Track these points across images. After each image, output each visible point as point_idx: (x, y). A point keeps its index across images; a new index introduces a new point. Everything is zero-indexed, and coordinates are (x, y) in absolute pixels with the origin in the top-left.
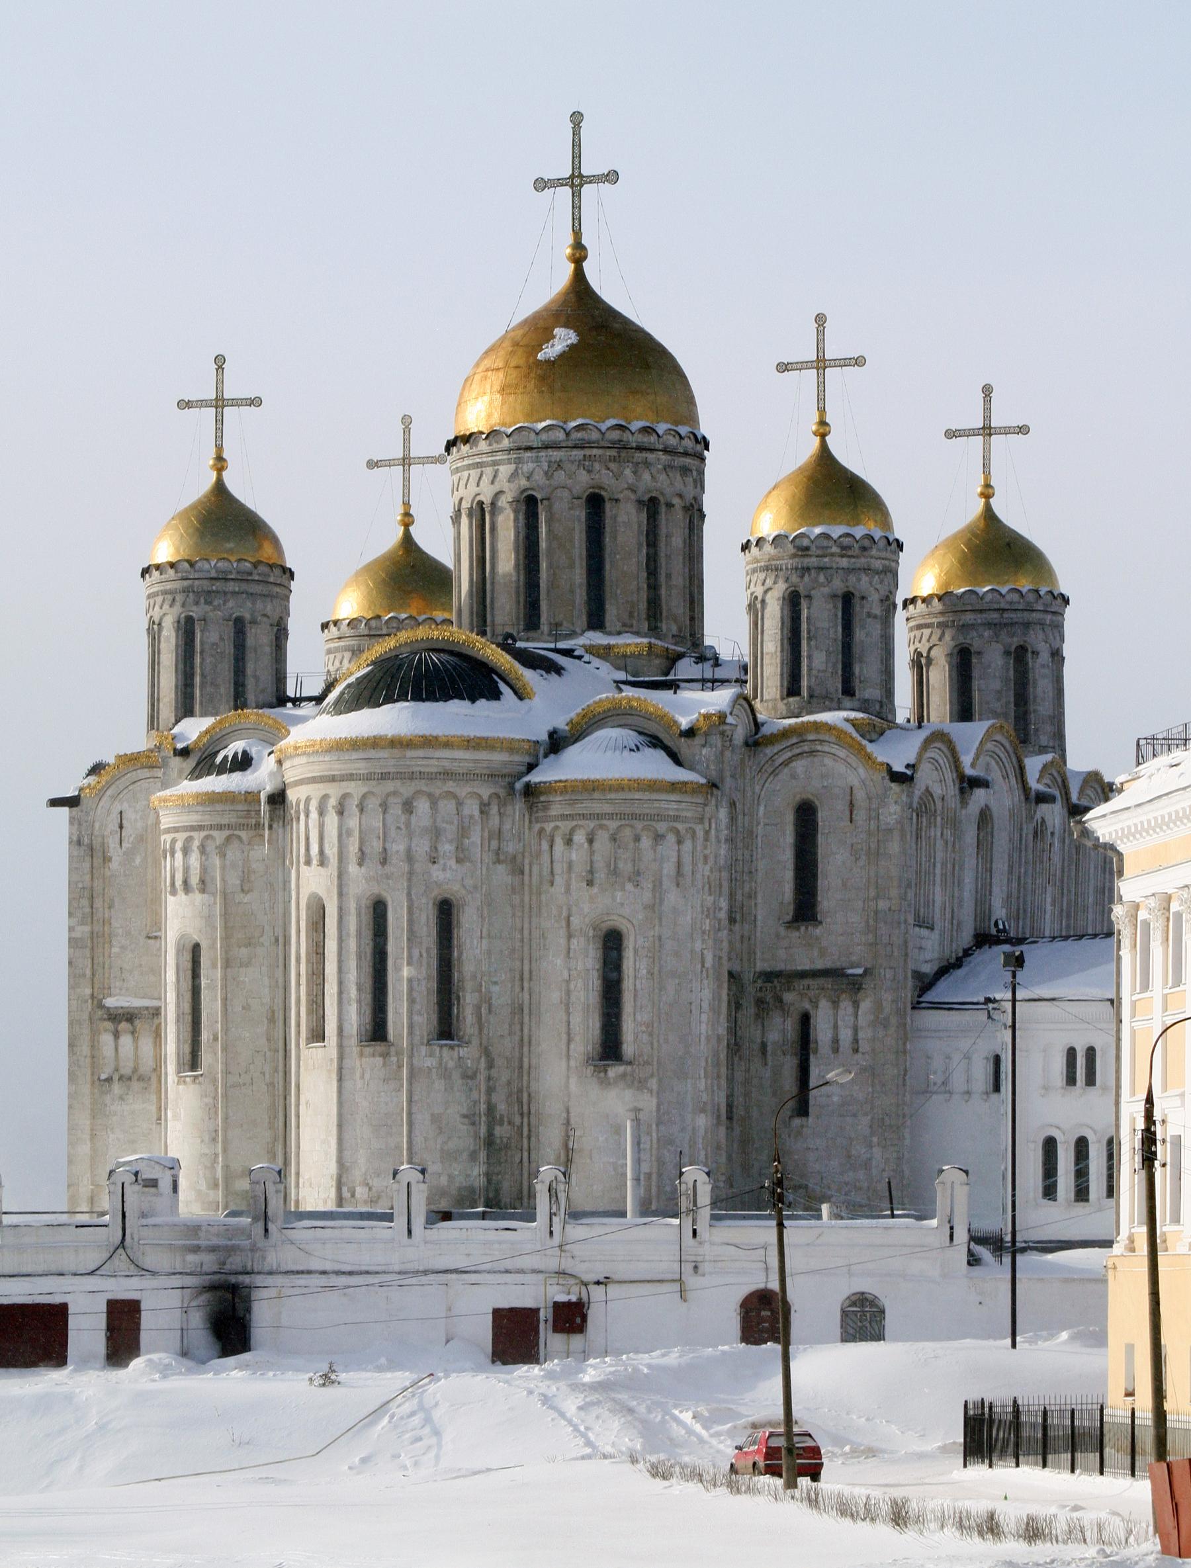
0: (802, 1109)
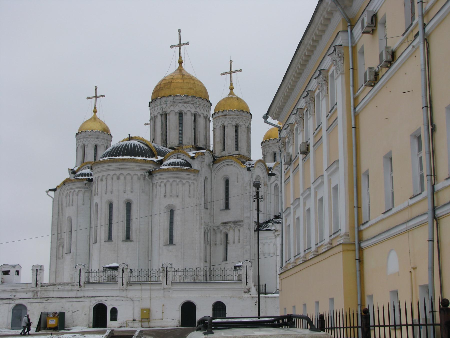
0: (226, 259)
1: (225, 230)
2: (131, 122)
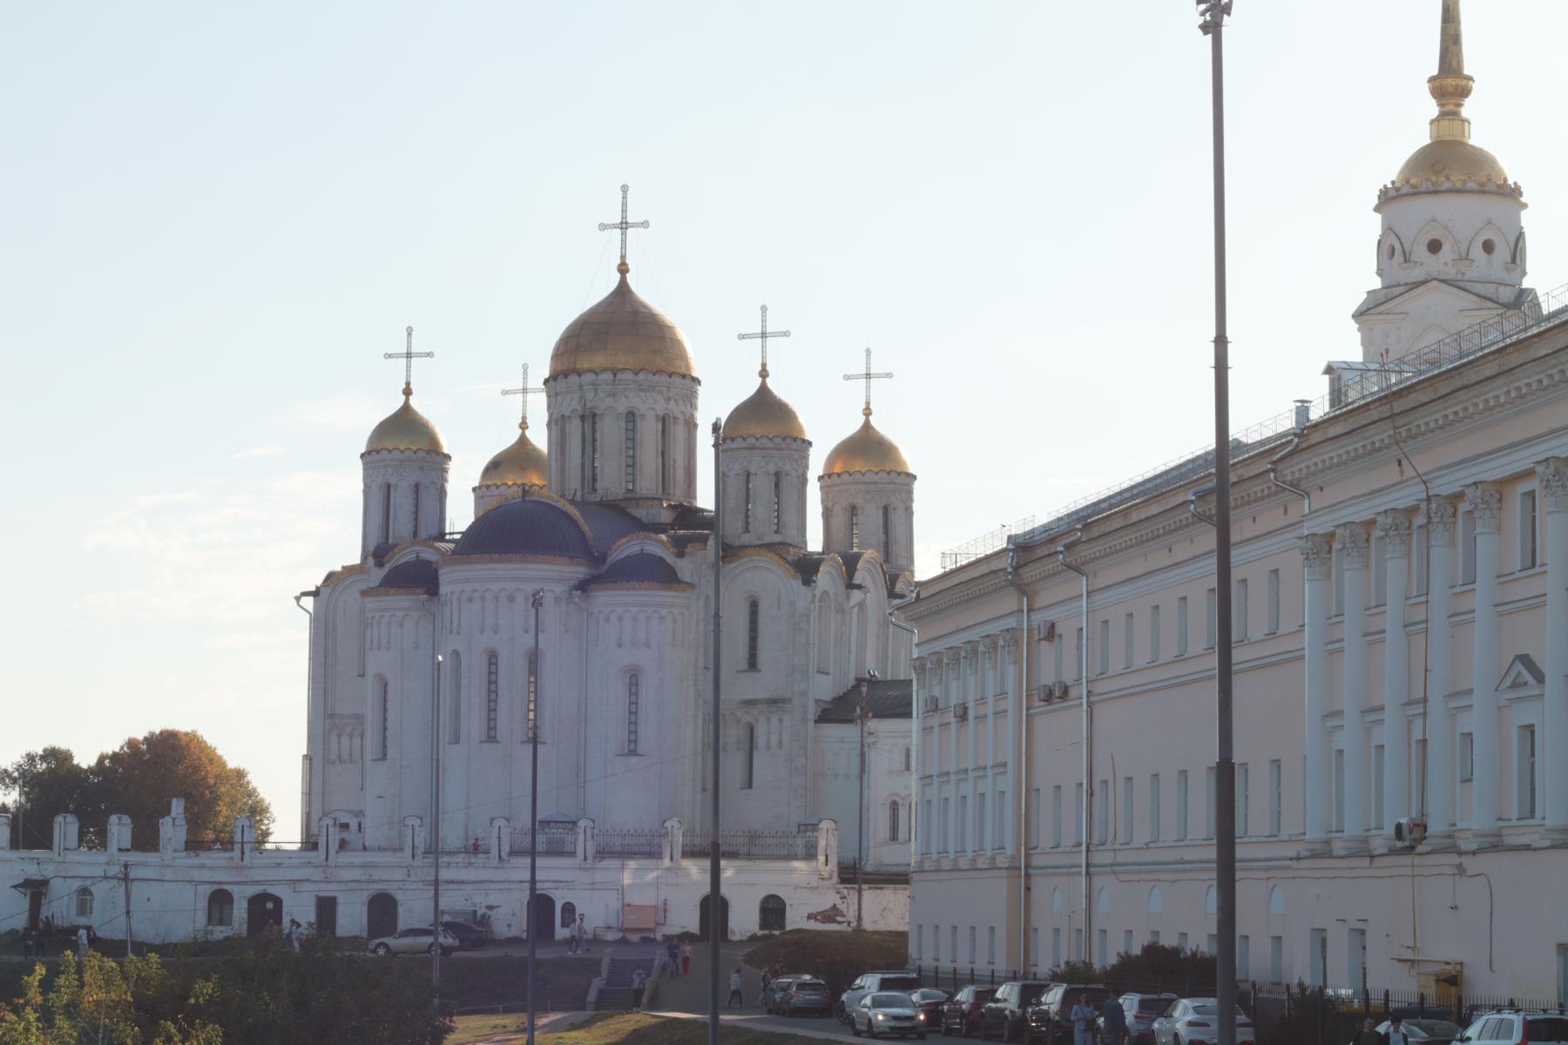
0: (750, 785)
1: (747, 719)
2: (489, 414)
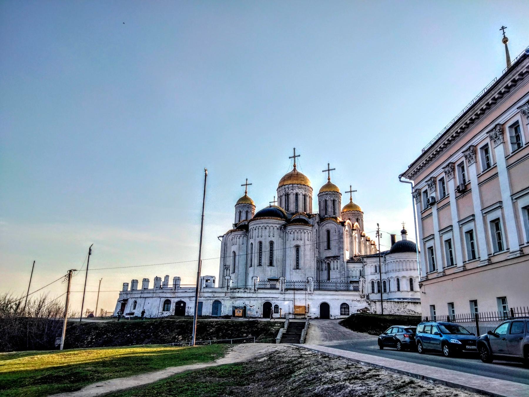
1: (328, 262)
